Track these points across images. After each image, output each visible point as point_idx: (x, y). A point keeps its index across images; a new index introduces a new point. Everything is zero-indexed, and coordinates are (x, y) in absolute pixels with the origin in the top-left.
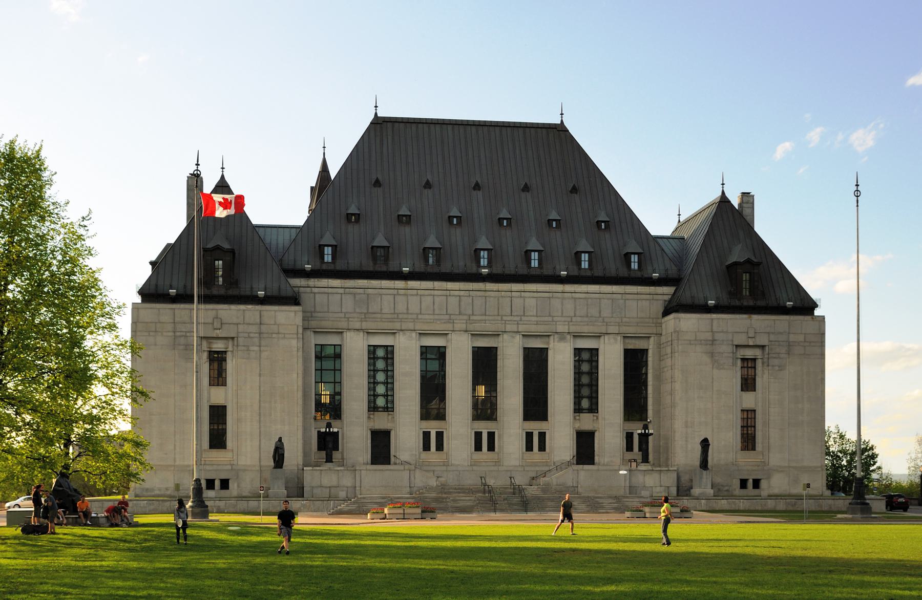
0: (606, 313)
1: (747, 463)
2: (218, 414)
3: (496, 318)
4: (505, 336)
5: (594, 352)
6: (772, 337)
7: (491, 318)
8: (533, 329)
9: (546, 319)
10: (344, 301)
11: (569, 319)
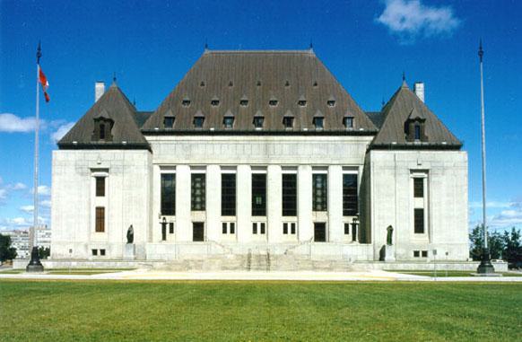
1: (420, 241)
2: (100, 213)
5: (324, 177)
6: (433, 165)
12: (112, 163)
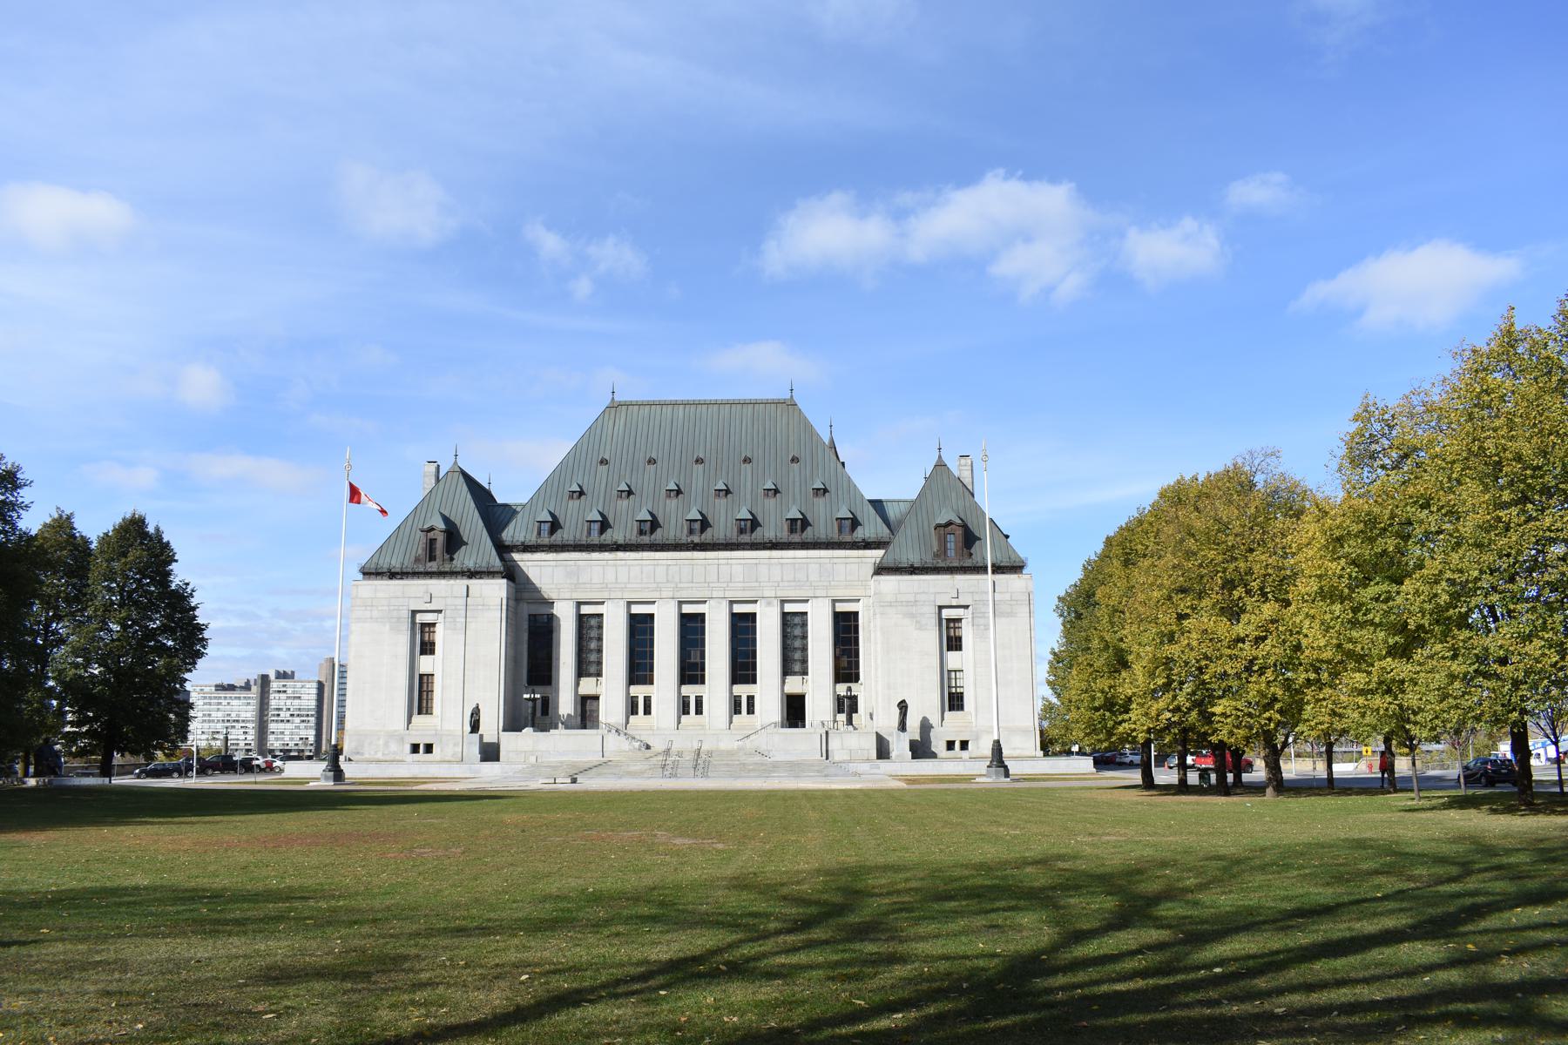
12: (449, 601)
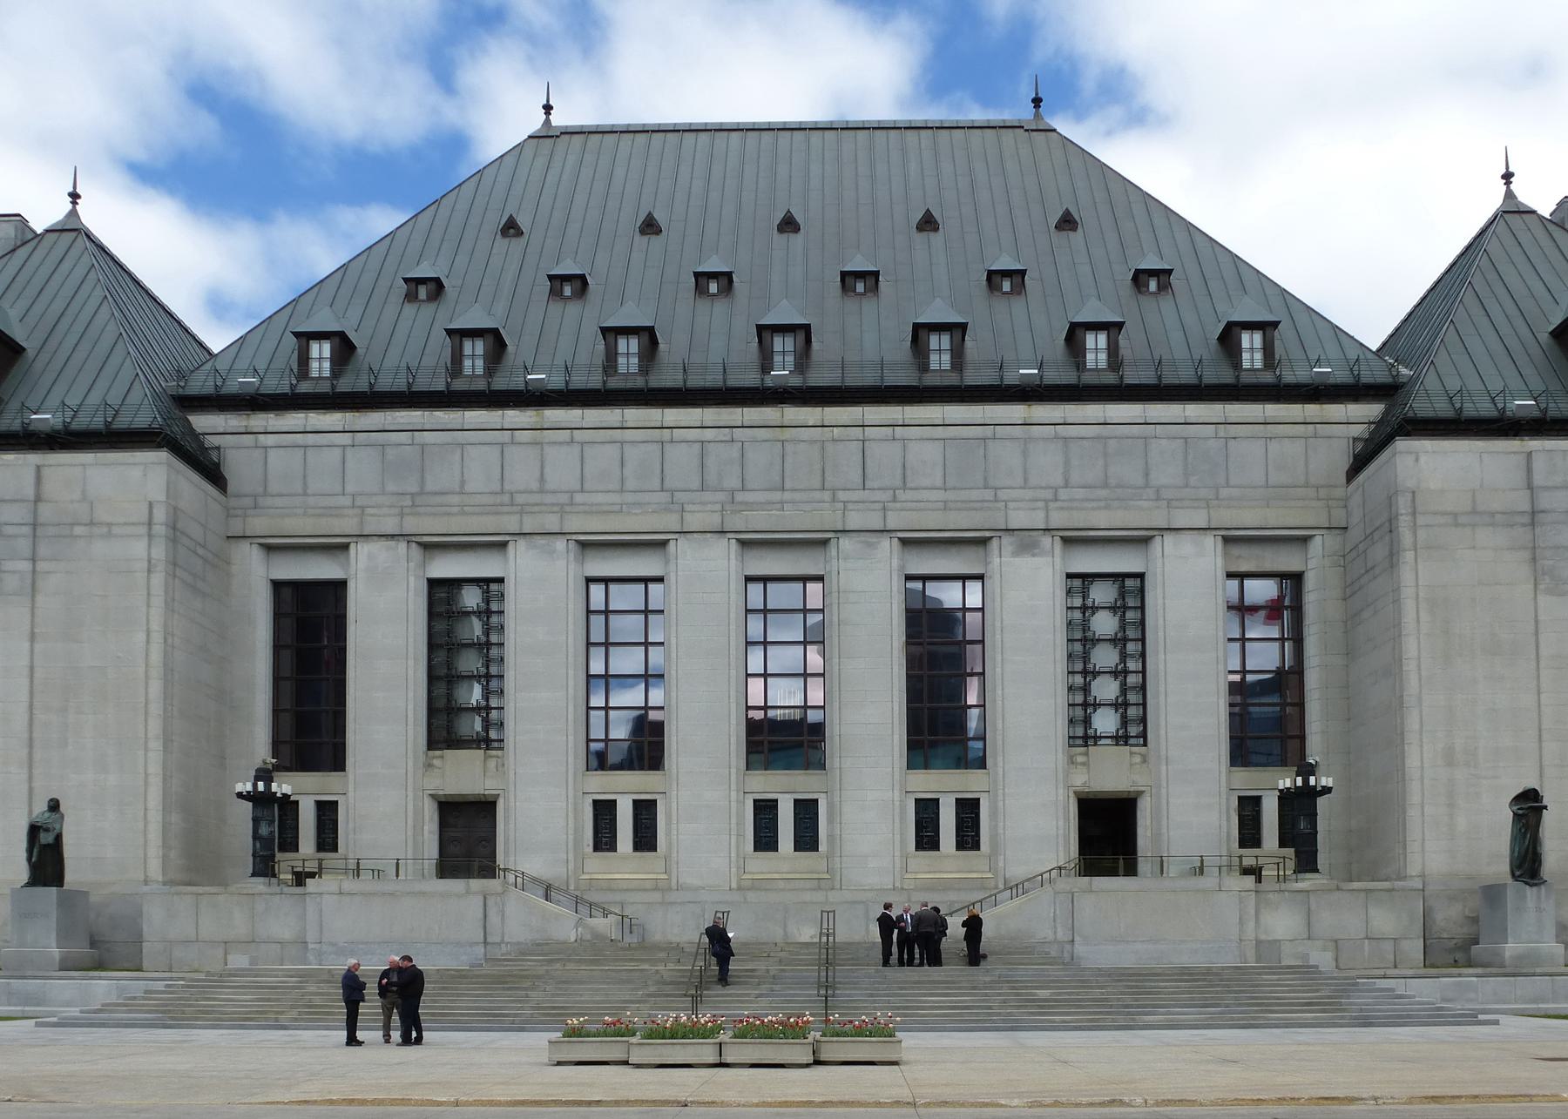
0: (1166, 474)
3: (817, 495)
4: (846, 543)
5: (1131, 588)
7: (797, 496)
8: (932, 521)
9: (975, 495)
10: (349, 465)
11: (1049, 494)
